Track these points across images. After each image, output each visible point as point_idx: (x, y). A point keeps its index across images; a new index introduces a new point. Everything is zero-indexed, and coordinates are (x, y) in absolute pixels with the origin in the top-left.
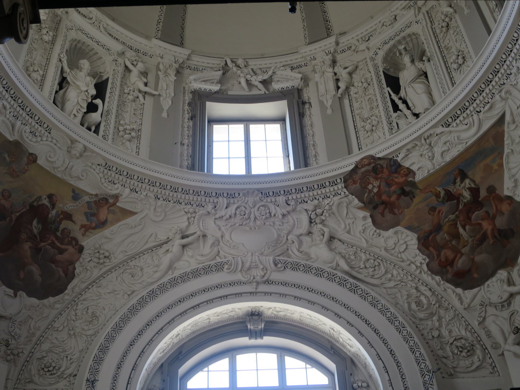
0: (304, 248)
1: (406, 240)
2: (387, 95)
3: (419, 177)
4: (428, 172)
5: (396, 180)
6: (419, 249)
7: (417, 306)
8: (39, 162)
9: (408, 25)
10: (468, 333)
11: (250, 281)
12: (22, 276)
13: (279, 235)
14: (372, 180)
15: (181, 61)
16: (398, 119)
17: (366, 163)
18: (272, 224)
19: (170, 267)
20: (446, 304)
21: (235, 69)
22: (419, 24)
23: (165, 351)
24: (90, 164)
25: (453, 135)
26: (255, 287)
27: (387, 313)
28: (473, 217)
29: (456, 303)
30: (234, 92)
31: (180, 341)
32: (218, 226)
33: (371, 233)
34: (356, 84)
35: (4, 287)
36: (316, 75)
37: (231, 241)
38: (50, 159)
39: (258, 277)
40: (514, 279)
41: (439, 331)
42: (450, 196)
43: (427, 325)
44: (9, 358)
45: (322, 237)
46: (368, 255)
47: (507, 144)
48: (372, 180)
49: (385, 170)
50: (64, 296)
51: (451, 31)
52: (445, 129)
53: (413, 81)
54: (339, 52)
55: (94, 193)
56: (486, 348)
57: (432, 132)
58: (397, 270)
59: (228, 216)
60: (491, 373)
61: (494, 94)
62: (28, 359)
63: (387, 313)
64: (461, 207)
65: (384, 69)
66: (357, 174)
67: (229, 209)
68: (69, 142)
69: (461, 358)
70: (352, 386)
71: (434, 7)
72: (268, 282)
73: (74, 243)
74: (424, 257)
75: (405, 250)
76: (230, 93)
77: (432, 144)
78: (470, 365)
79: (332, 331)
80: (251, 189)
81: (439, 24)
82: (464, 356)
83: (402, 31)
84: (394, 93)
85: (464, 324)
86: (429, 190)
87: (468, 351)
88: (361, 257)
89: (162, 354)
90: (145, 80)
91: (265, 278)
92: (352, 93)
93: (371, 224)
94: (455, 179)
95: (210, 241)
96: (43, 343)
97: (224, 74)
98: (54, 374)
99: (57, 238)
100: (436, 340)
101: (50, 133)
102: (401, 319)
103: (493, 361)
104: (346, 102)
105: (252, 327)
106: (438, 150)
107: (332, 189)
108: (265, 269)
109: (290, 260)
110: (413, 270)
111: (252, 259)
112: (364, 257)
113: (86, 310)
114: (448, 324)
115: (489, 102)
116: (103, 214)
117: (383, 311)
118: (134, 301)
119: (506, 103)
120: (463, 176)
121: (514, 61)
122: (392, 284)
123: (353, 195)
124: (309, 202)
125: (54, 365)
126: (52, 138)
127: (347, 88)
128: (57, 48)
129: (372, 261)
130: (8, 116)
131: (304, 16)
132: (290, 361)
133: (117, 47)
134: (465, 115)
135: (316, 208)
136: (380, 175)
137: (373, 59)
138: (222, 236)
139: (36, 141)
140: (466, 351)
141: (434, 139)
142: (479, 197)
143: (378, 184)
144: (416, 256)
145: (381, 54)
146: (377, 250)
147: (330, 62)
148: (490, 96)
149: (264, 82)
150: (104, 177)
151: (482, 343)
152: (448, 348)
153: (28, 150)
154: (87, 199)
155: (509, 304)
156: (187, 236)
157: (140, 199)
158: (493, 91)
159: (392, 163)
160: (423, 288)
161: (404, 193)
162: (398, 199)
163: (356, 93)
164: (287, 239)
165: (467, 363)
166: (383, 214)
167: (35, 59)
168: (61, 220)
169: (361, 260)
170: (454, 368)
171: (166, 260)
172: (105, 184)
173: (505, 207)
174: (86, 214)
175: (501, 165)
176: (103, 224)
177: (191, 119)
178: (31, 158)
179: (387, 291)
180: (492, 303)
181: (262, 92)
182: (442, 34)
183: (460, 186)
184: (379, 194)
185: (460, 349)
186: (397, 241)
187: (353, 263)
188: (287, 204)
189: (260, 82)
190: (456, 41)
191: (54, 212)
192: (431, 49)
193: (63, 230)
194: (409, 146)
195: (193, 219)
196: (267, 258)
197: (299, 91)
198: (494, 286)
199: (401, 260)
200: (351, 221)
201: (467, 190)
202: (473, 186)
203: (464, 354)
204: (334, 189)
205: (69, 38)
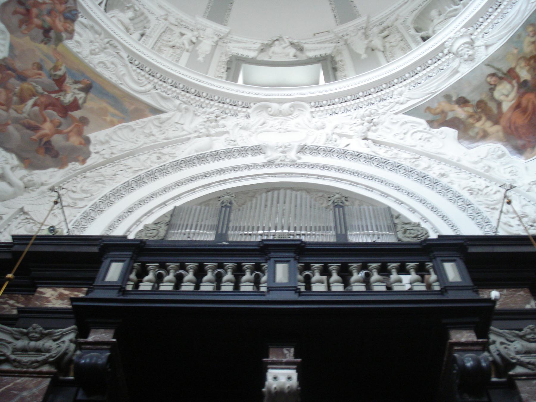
5: (57, 21)
22: (157, 21)
28: (50, 111)
42: (60, 81)
47: (137, 123)
52: (127, 59)
57: (119, 47)
64: (54, 95)
86: (58, 58)
106: (102, 57)
119: (175, 111)
120: (87, 89)
134: (147, 76)
141: (110, 50)
142: (72, 111)
148: (174, 94)
159: (74, 12)
161: (47, 31)
173: (75, 140)
175: (112, 124)
183: (75, 88)
194: (96, 27)
202: (80, 102)
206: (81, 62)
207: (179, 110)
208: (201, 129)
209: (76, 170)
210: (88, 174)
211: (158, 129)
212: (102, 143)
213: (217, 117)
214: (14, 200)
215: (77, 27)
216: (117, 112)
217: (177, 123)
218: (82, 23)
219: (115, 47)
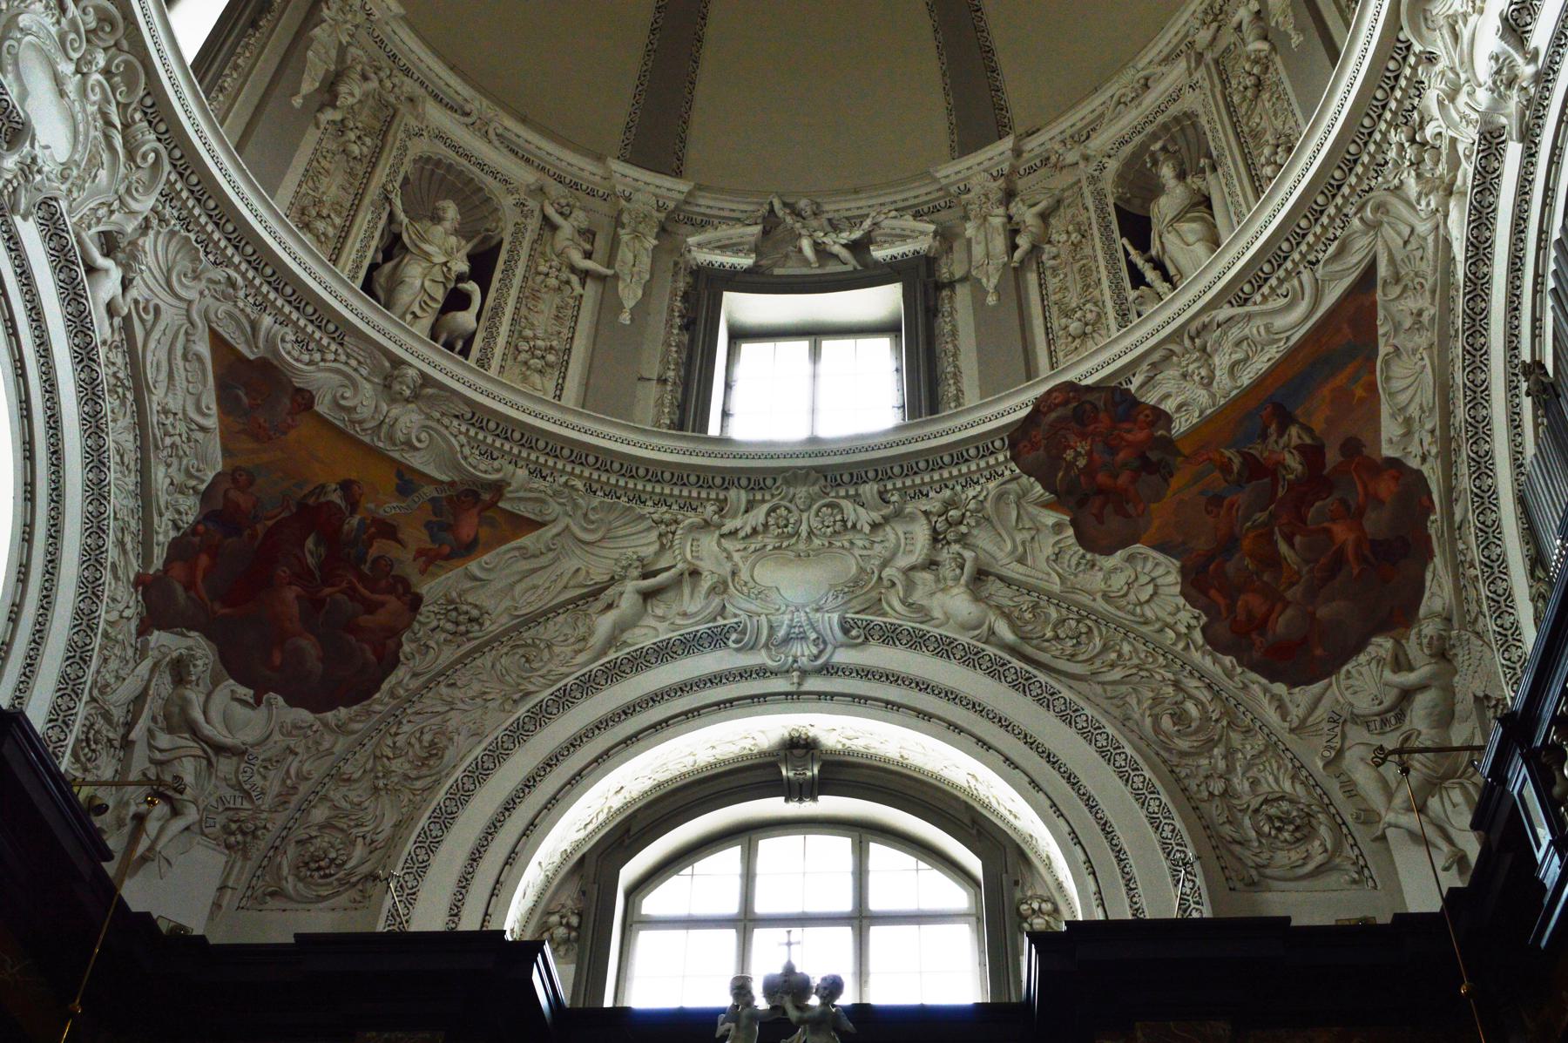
0: (918, 596)
1: (1154, 575)
2: (1121, 255)
3: (1180, 425)
4: (1201, 413)
5: (1129, 437)
6: (1183, 593)
7: (1175, 724)
8: (319, 408)
9: (1174, 96)
10: (1298, 787)
11: (785, 668)
12: (277, 659)
13: (862, 570)
14: (1072, 439)
15: (672, 205)
16: (1141, 304)
18: (847, 544)
19: (612, 641)
20: (1248, 720)
21: (789, 220)
22: (1197, 90)
23: (590, 828)
24: (437, 415)
26: (795, 680)
27: (1099, 737)
29: (1271, 715)
30: (791, 269)
31: (627, 805)
32: (725, 550)
33: (1074, 562)
34: (1055, 237)
35: (232, 681)
36: (968, 225)
37: (751, 584)
38: (343, 402)
39: (805, 659)
40: (1411, 657)
41: (1228, 780)
42: (1256, 469)
43: (1198, 766)
44: (232, 839)
45: (958, 571)
46: (1064, 612)
47: (1384, 335)
48: (1072, 439)
49: (1102, 415)
50: (370, 705)
51: (1265, 96)
53: (1179, 218)
54: (1022, 172)
55: (444, 478)
56: (1344, 823)
57: (1206, 319)
58: (1133, 645)
59: (748, 529)
60: (1354, 882)
61: (1346, 215)
62: (278, 843)
63: (1099, 737)
64: (1280, 493)
65: (1119, 198)
67: (752, 514)
68: (387, 364)
69: (1280, 844)
70: (1018, 909)
71: (1232, 47)
72: (828, 670)
73: (400, 588)
74: (1197, 612)
75: (1152, 596)
76: (778, 271)
77: (1209, 349)
78: (1300, 862)
79: (973, 783)
81: (1239, 83)
82: (1286, 841)
83: (1160, 111)
84: (1136, 248)
85: (1290, 765)
87: (1297, 828)
88: (1047, 616)
89: (582, 834)
90: (588, 247)
91: (820, 662)
92: (1045, 257)
93: (1073, 540)
94: (1266, 427)
95: (706, 584)
96: (314, 807)
97: (765, 232)
98: (331, 875)
99: (362, 577)
100: (1217, 801)
101: (342, 344)
102: (1129, 750)
103: (1362, 855)
104: (1032, 278)
105: (791, 774)
106: (1221, 361)
107: (983, 464)
108: (821, 641)
109: (879, 620)
110: (1169, 642)
111: (792, 620)
112: (1054, 615)
113: (418, 735)
114: (1249, 766)
115: (1336, 238)
116: (468, 527)
117: (1089, 733)
118: (521, 711)
120: (1285, 419)
121: (1392, 131)
122: (1117, 674)
123: (1030, 476)
124: (932, 494)
125: (333, 855)
126: (348, 355)
127: (1035, 249)
128: (380, 176)
129: (1073, 623)
130: (241, 304)
131: (952, 101)
132: (879, 852)
133: (525, 176)
134: (1281, 273)
135: (949, 505)
136: (1092, 427)
137: (1093, 180)
138: (734, 574)
140: (1291, 827)
142: (1323, 465)
143: (1087, 448)
144: (1178, 609)
145: (1113, 165)
146: (1085, 599)
147: (1000, 194)
149: (853, 246)
150: (469, 443)
151: (1333, 810)
152: (1247, 822)
153: (291, 382)
154: (429, 491)
155: (1400, 718)
156: (655, 574)
158: (1345, 211)
159: (1118, 398)
160: (1192, 684)
161: (1147, 466)
163: (1054, 258)
164: (880, 578)
165: (1295, 856)
166: (1100, 518)
167: (324, 193)
168: (371, 539)
169: (1047, 621)
170: (1258, 867)
171: (604, 624)
172: (474, 462)
173: (1385, 488)
174: (429, 526)
175: (1372, 388)
176: (468, 549)
177: (687, 329)
179: (1105, 691)
180: (1357, 716)
181: (849, 268)
182: (1245, 106)
183: (1276, 442)
184: (1090, 470)
185: (1278, 824)
186: (1133, 577)
187: (1030, 627)
188: (883, 500)
189: (844, 246)
190: (1275, 114)
191: (355, 521)
192: (1220, 138)
193: (376, 561)
194: (1156, 357)
195: (670, 536)
196: (827, 615)
198: (1361, 674)
199: (1142, 620)
200: (1027, 535)
202: (1308, 441)
203: (1286, 835)
204: (987, 463)
205: (412, 154)
206: (1221, 412)
207: (1373, 227)
208: (1428, 204)
212: (1408, 434)
214: (1459, 696)
215: (1151, 398)
216: (1349, 370)
217: (1406, 243)
218: (1142, 386)
219: (1205, 326)
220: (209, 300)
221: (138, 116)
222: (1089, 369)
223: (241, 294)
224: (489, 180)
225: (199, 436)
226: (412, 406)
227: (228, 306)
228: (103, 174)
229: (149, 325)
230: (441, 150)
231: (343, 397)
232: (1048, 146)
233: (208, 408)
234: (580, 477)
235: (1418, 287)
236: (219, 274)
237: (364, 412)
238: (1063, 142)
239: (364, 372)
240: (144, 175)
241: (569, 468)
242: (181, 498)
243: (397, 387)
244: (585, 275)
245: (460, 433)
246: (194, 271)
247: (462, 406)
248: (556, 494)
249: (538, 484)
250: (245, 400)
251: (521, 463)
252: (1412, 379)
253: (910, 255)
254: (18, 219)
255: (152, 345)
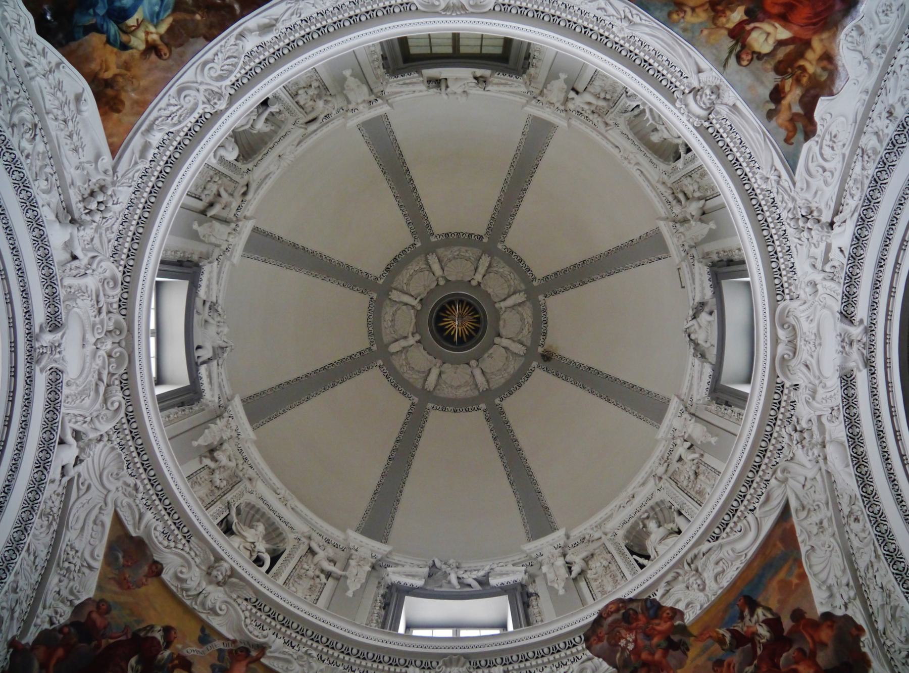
3: (690, 617)
4: (701, 606)
5: (658, 628)
8: (163, 576)
14: (623, 632)
15: (379, 557)
17: (612, 610)
22: (662, 491)
25: (725, 550)
38: (180, 575)
42: (740, 639)
48: (623, 632)
49: (640, 616)
52: (713, 544)
55: (231, 637)
57: (695, 551)
64: (759, 652)
66: (602, 626)
68: (212, 558)
77: (700, 570)
80: (455, 655)
86: (708, 636)
92: (588, 576)
94: (742, 612)
101: (188, 541)
104: (583, 584)
106: (708, 575)
115: (763, 493)
120: (752, 604)
121: (783, 430)
123: (599, 657)
126: (191, 549)
130: (138, 501)
134: (735, 519)
136: (634, 625)
139: (168, 546)
141: (699, 563)
142: (783, 630)
143: (634, 637)
145: (621, 533)
148: (763, 485)
150: (250, 617)
153: (152, 556)
154: (219, 644)
157: (295, 656)
161: (672, 645)
162: (665, 654)
173: (825, 635)
175: (803, 576)
177: (384, 609)
178: (154, 568)
183: (750, 620)
184: (636, 651)
189: (475, 579)
191: (167, 653)
194: (669, 577)
197: (523, 586)
201: (763, 625)
202: (770, 616)
206: (713, 605)
207: (784, 481)
208: (813, 454)
209: (873, 643)
210: (880, 626)
211: (812, 513)
212: (831, 596)
213: (796, 430)
215: (668, 603)
216: (785, 569)
217: (804, 486)
218: (663, 595)
219: (696, 556)
220: (120, 494)
221: (117, 382)
222: (629, 590)
223: (140, 495)
224: (283, 525)
225: (86, 571)
226: (221, 588)
227: (130, 501)
228: (87, 401)
229: (82, 492)
230: (260, 504)
231: (181, 572)
232: (584, 532)
233: (98, 556)
234: (316, 649)
235: (816, 508)
236: (131, 481)
237: (191, 584)
238: (592, 529)
239: (197, 560)
240: (109, 414)
241: (310, 643)
242: (61, 605)
243: (215, 573)
244: (329, 575)
245: (247, 610)
246: (117, 474)
247: (251, 593)
248: (299, 658)
249: (288, 649)
250: (121, 560)
251: (279, 636)
252: (826, 562)
253: (512, 583)
254: (38, 369)
255: (78, 504)
